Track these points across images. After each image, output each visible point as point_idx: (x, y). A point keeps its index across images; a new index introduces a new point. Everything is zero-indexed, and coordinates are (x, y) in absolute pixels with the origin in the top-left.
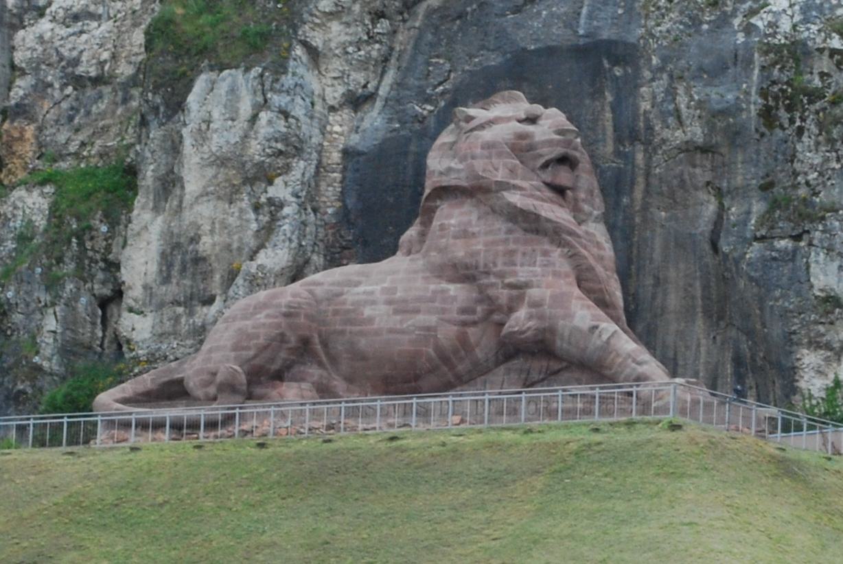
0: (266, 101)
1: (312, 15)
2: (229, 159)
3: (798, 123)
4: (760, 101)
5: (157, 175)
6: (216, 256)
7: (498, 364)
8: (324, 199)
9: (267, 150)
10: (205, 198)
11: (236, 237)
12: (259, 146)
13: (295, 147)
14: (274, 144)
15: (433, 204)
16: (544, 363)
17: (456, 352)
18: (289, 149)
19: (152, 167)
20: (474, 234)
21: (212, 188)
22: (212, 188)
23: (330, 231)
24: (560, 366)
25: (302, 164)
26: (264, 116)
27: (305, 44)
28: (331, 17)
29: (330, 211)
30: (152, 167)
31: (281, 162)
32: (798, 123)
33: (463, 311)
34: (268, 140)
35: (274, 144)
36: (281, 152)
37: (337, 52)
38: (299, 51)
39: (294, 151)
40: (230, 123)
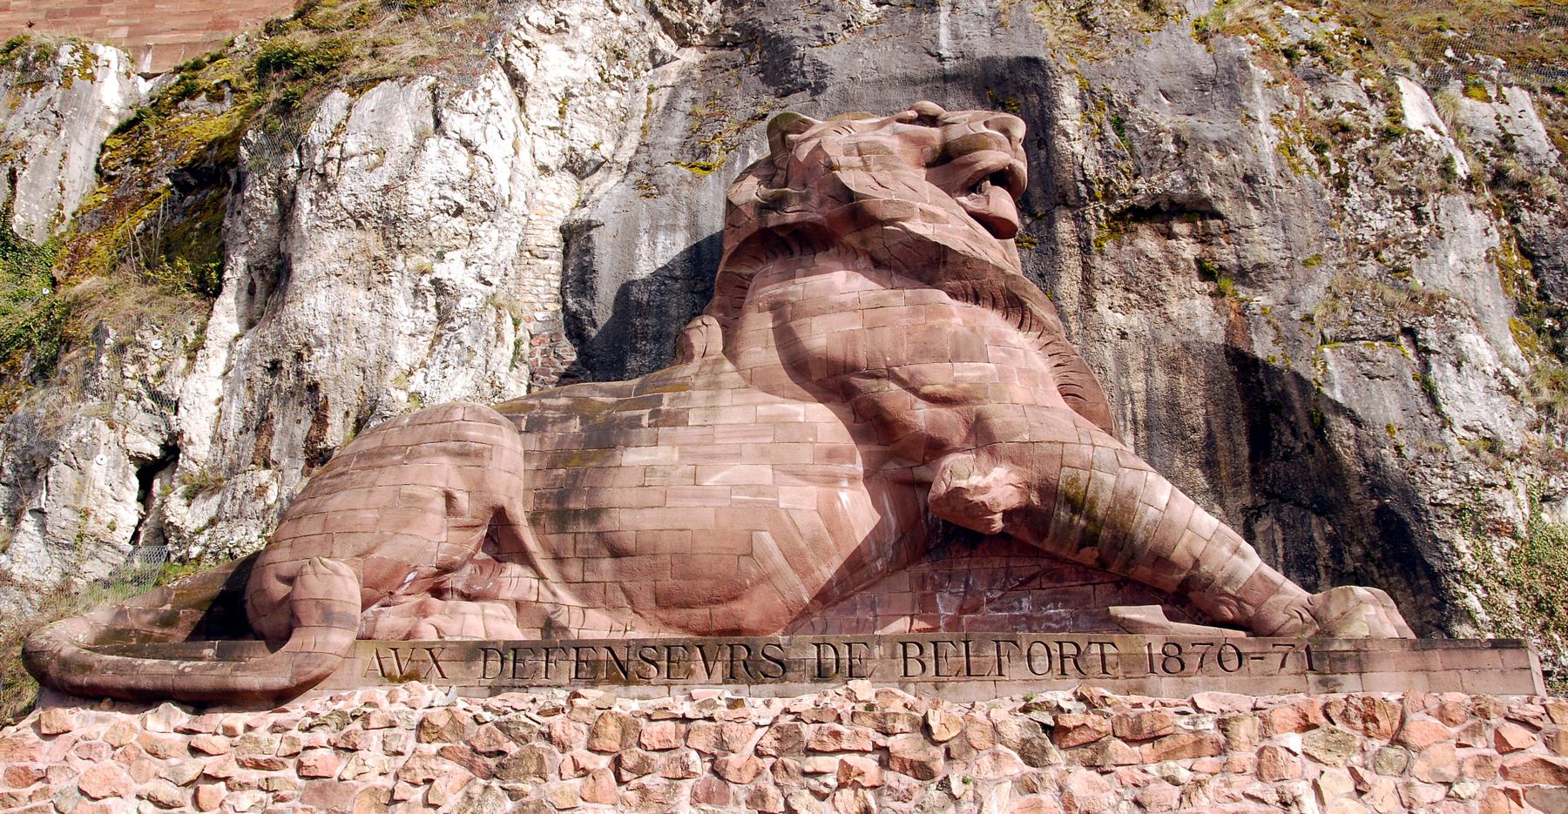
0: (438, 123)
1: (519, 26)
2: (367, 216)
3: (1335, 169)
4: (1273, 131)
5: (252, 260)
6: (337, 379)
7: (896, 566)
8: (531, 298)
9: (436, 202)
10: (324, 283)
11: (371, 346)
12: (421, 192)
13: (483, 204)
14: (448, 192)
15: (745, 271)
16: (997, 563)
17: (815, 543)
18: (474, 206)
19: (245, 248)
20: (841, 304)
21: (336, 265)
22: (336, 265)
23: (539, 349)
24: (1037, 569)
25: (494, 233)
26: (433, 144)
27: (507, 66)
28: (547, 37)
29: (540, 316)
30: (245, 248)
31: (459, 223)
32: (1335, 169)
33: (832, 455)
34: (440, 184)
35: (448, 192)
36: (459, 211)
37: (556, 91)
38: (498, 72)
39: (482, 213)
40: (374, 157)
